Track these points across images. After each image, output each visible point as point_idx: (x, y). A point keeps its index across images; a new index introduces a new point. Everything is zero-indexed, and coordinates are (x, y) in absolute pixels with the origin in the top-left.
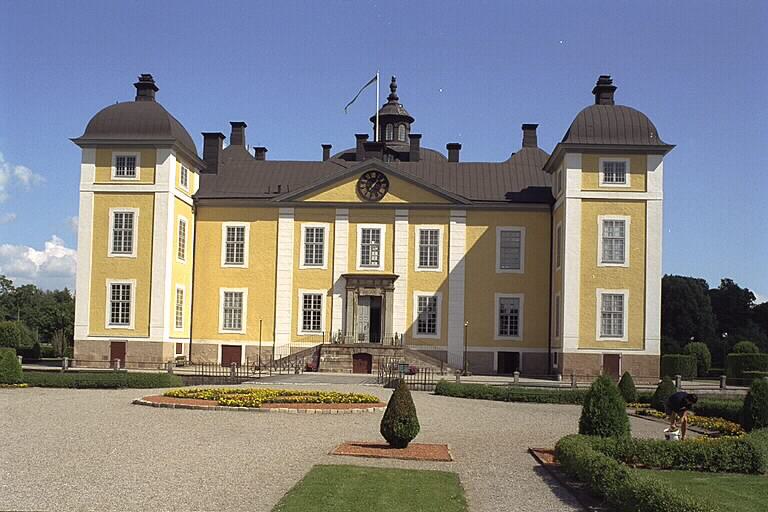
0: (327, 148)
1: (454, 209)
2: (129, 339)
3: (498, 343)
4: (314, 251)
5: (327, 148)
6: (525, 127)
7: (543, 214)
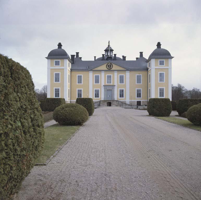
0: (95, 57)
1: (127, 71)
3: (136, 99)
4: (97, 80)
5: (95, 57)
6: (140, 53)
7: (146, 72)
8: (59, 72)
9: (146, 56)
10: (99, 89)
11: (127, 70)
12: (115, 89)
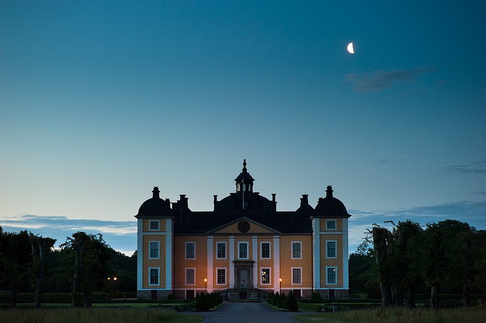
0: (215, 197)
2: (158, 289)
3: (293, 286)
4: (222, 253)
5: (215, 197)
7: (309, 236)
9: (313, 203)
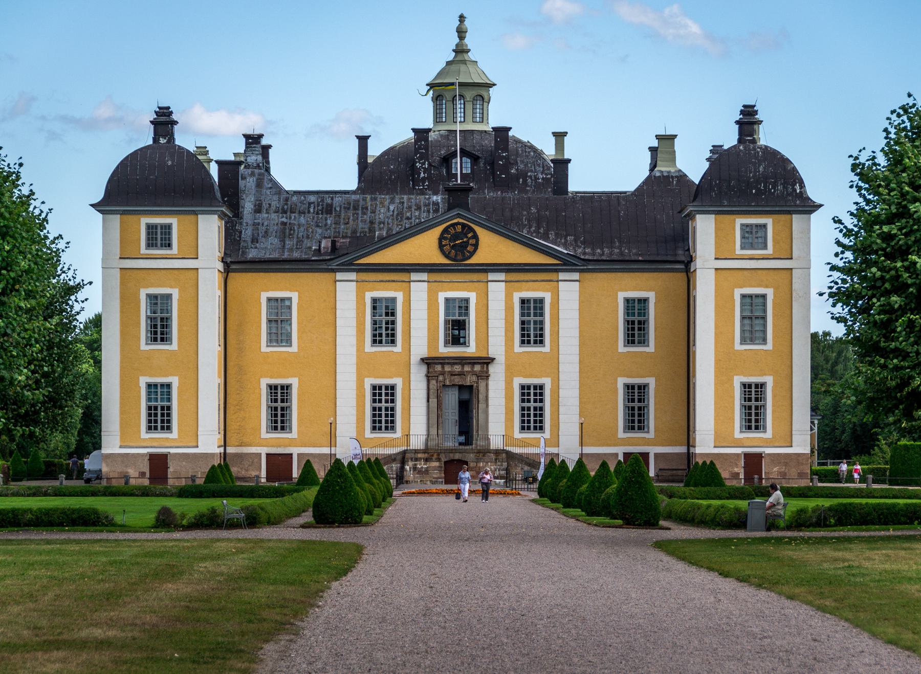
0: (363, 141)
2: (172, 451)
3: (624, 442)
5: (363, 141)
8: (171, 287)
10: (398, 382)
11: (567, 264)
12: (491, 383)
